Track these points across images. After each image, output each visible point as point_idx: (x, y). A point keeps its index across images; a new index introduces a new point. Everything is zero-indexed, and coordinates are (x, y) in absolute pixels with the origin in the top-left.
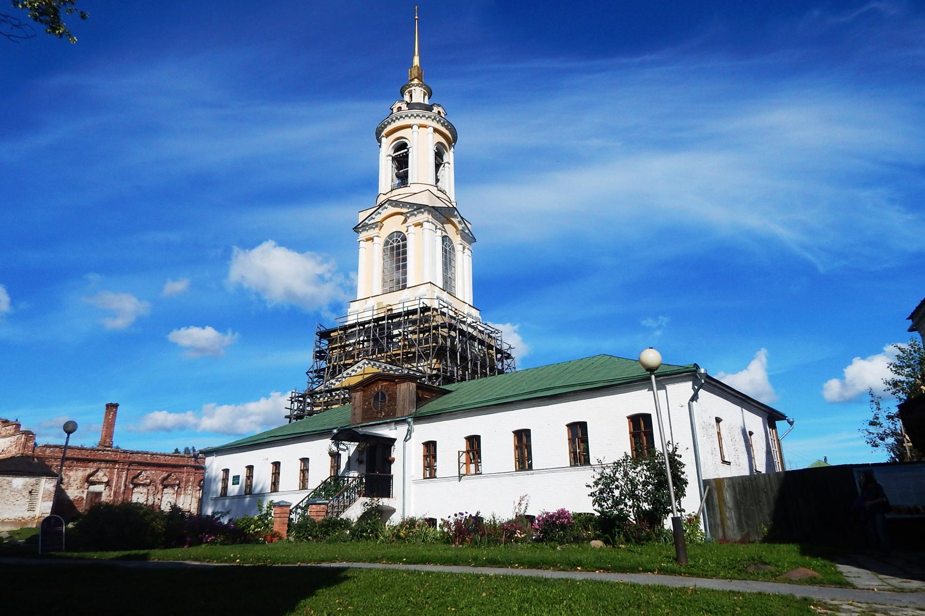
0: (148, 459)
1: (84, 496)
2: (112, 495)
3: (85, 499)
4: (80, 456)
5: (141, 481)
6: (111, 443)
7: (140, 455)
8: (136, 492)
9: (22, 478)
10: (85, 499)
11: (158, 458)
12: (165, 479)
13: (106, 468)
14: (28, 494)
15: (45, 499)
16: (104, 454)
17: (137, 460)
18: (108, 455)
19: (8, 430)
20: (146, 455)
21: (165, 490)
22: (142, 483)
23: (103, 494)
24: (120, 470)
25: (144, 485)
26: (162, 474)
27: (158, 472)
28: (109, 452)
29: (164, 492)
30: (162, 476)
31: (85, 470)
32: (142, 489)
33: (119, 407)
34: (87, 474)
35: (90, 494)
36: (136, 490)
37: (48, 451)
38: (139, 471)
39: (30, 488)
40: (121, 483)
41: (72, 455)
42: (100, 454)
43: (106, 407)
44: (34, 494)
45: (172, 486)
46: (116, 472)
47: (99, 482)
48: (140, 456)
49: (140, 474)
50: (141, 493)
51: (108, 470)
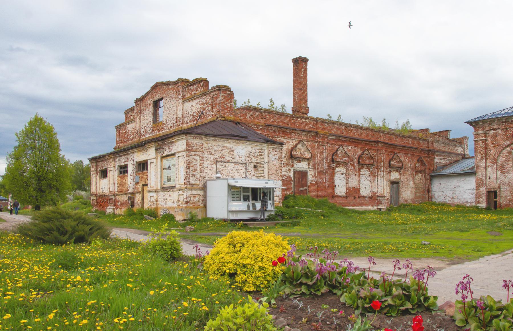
0: (343, 131)
1: (291, 175)
2: (316, 175)
3: (292, 179)
4: (280, 124)
5: (341, 159)
6: (307, 109)
7: (336, 126)
8: (339, 172)
9: (244, 147)
10: (292, 179)
11: (352, 130)
12: (359, 158)
13: (307, 141)
14: (253, 169)
15: (273, 177)
16: (303, 122)
17: (333, 132)
18: (307, 124)
19: (193, 90)
20: (340, 127)
21: (362, 170)
22: (341, 161)
23: (309, 174)
24: (321, 144)
25: (344, 164)
26: (358, 151)
27: (354, 148)
28: (307, 121)
29: (362, 173)
30: (358, 154)
31: (288, 142)
32: (342, 169)
33: (308, 63)
34: (290, 148)
35: (296, 174)
36: (337, 170)
37: (249, 115)
38: (337, 147)
39: (255, 160)
40: (323, 160)
41: (273, 122)
42: (300, 122)
43: (292, 64)
44: (260, 169)
45: (368, 166)
46: (316, 147)
47: (303, 158)
48: (336, 128)
49: (337, 151)
50: (342, 174)
51: (309, 143)
